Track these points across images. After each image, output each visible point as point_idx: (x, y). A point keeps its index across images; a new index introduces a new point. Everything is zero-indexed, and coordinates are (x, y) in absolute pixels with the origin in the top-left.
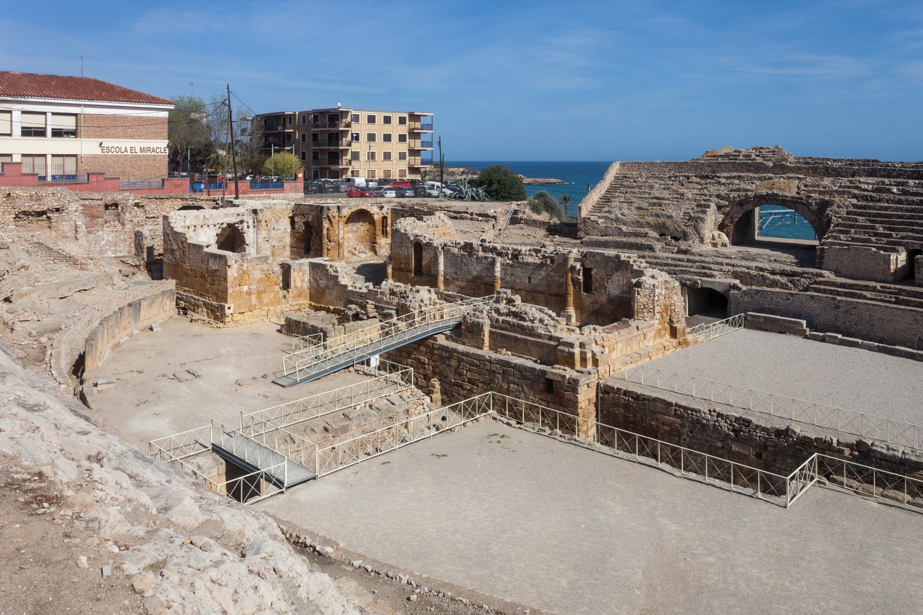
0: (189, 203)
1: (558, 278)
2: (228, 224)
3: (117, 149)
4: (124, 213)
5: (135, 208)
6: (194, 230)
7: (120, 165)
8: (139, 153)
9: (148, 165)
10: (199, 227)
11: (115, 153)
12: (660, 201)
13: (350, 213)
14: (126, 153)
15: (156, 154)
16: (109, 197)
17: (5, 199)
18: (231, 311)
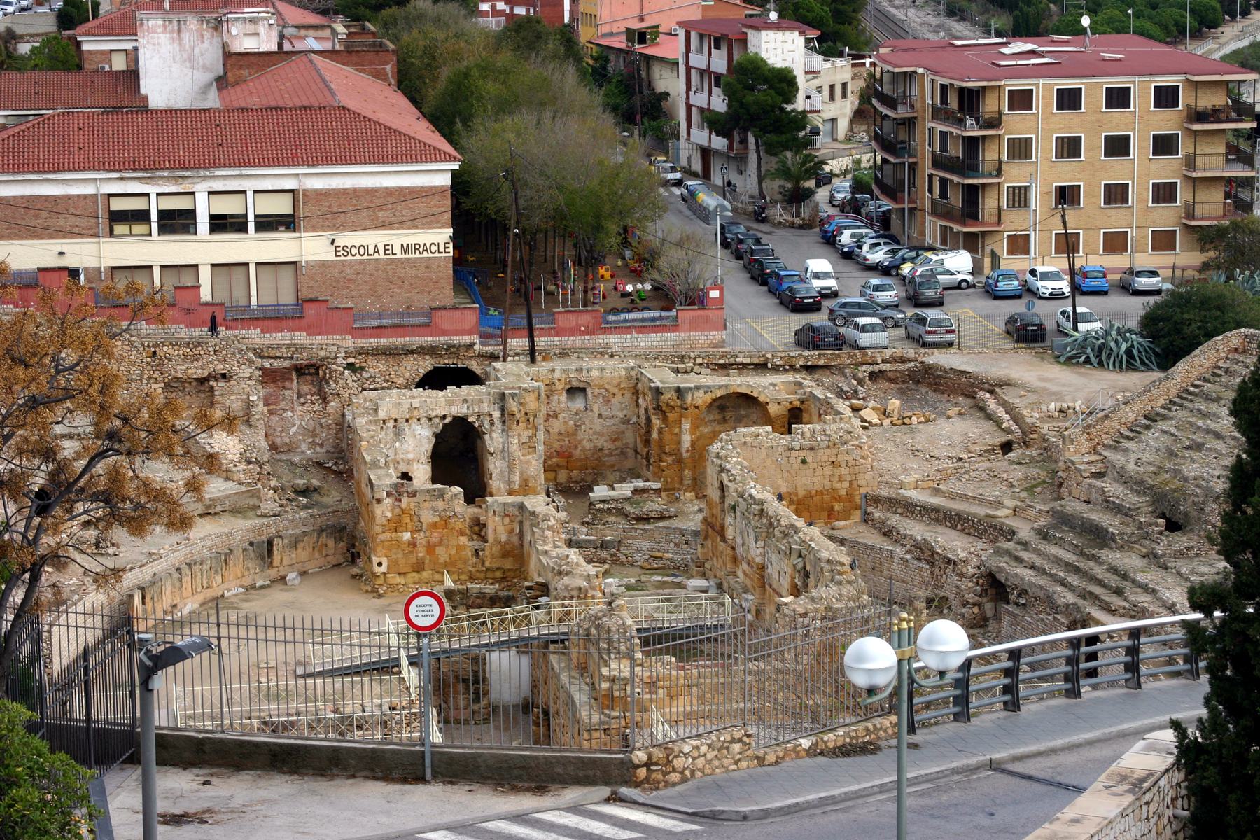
0: (446, 361)
3: (362, 249)
4: (327, 382)
5: (347, 372)
6: (394, 427)
7: (367, 278)
8: (399, 256)
9: (417, 277)
10: (402, 423)
11: (358, 257)
13: (709, 401)
14: (376, 256)
15: (430, 255)
16: (305, 354)
17: (149, 360)
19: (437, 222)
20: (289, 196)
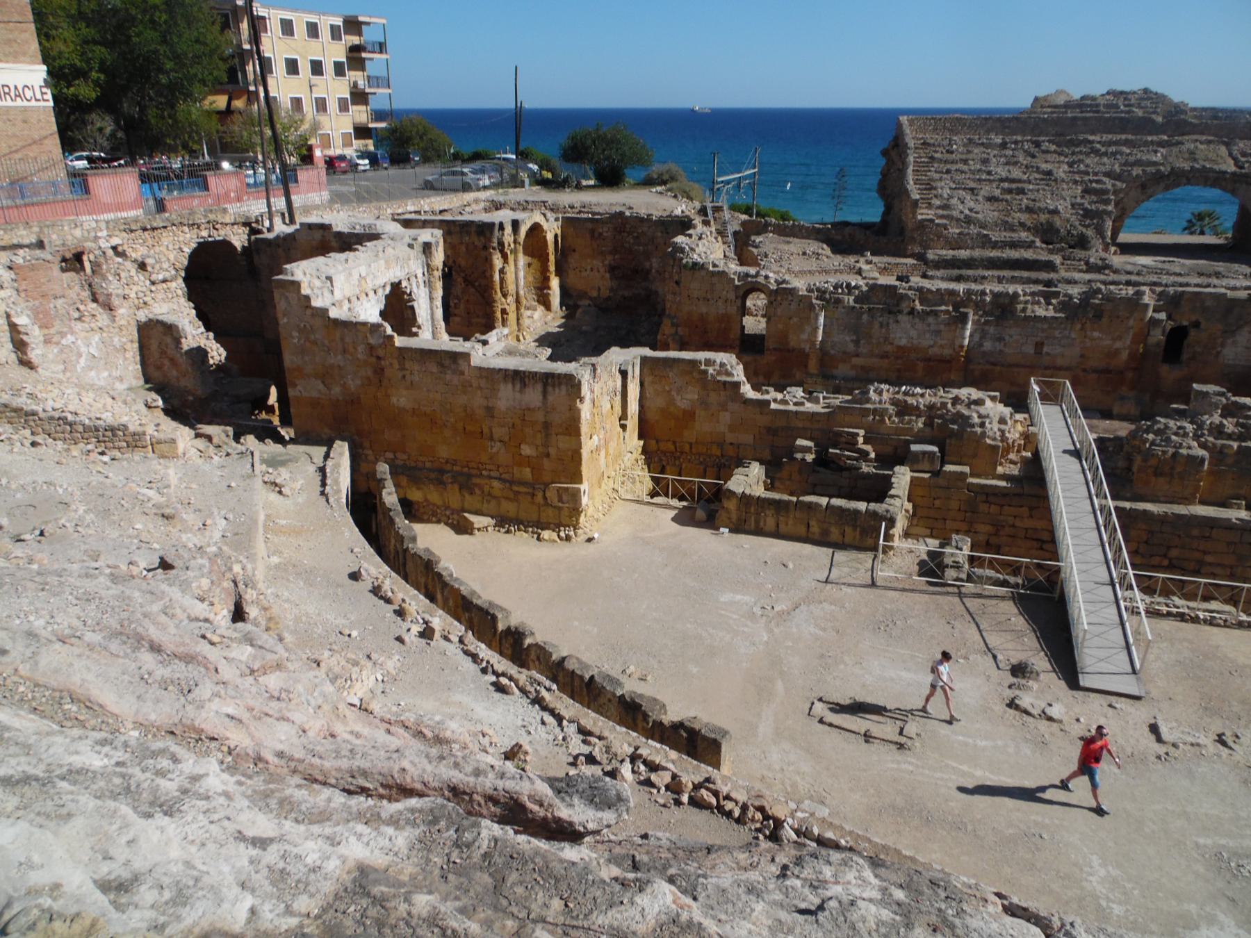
1: (1108, 342)
2: (392, 284)
9: (15, 136)
12: (1020, 185)
15: (26, 103)
19: (24, 54)
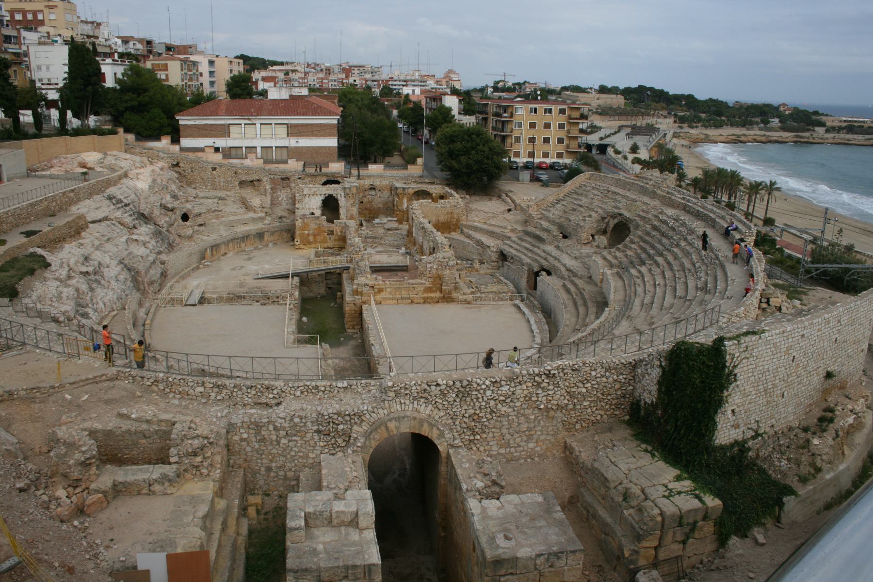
18: (298, 243)
20: (286, 126)
